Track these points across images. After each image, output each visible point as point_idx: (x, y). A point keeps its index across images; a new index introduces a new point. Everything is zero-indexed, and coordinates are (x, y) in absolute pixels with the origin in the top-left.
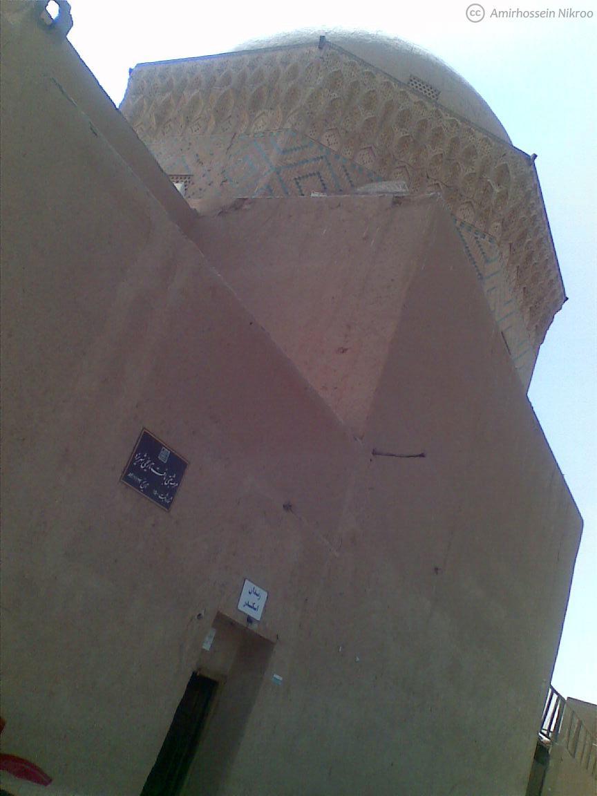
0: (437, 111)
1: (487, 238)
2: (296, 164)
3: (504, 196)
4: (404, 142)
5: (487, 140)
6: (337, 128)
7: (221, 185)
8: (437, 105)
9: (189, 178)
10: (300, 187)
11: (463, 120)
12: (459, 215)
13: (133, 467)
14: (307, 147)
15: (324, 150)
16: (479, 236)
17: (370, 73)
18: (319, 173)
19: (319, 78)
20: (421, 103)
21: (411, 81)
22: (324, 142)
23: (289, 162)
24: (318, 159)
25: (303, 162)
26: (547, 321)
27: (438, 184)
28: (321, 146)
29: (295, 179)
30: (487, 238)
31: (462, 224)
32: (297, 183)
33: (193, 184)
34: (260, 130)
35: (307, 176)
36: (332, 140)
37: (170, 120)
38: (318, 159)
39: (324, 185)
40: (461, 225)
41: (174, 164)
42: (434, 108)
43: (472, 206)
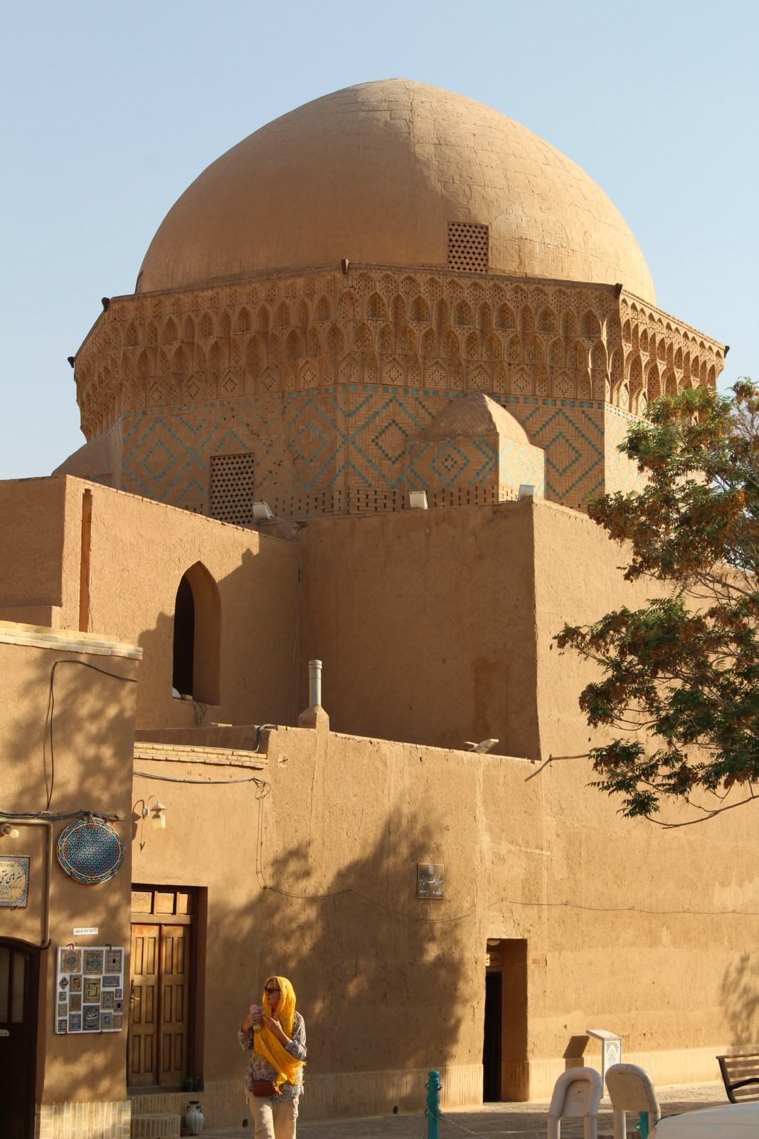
0: (495, 285)
2: (367, 424)
5: (560, 291)
6: (394, 359)
7: (294, 464)
8: (494, 277)
9: (250, 456)
10: (380, 448)
12: (557, 393)
14: (371, 396)
15: (390, 390)
16: (585, 408)
17: (409, 278)
18: (394, 421)
19: (356, 309)
21: (451, 230)
22: (387, 381)
23: (361, 423)
24: (388, 404)
25: (374, 417)
27: (522, 368)
29: (373, 441)
32: (377, 444)
33: (258, 464)
34: (311, 385)
35: (384, 431)
36: (394, 374)
37: (192, 376)
38: (388, 404)
39: (404, 432)
40: (562, 405)
41: (224, 440)
42: (492, 283)
43: (567, 375)
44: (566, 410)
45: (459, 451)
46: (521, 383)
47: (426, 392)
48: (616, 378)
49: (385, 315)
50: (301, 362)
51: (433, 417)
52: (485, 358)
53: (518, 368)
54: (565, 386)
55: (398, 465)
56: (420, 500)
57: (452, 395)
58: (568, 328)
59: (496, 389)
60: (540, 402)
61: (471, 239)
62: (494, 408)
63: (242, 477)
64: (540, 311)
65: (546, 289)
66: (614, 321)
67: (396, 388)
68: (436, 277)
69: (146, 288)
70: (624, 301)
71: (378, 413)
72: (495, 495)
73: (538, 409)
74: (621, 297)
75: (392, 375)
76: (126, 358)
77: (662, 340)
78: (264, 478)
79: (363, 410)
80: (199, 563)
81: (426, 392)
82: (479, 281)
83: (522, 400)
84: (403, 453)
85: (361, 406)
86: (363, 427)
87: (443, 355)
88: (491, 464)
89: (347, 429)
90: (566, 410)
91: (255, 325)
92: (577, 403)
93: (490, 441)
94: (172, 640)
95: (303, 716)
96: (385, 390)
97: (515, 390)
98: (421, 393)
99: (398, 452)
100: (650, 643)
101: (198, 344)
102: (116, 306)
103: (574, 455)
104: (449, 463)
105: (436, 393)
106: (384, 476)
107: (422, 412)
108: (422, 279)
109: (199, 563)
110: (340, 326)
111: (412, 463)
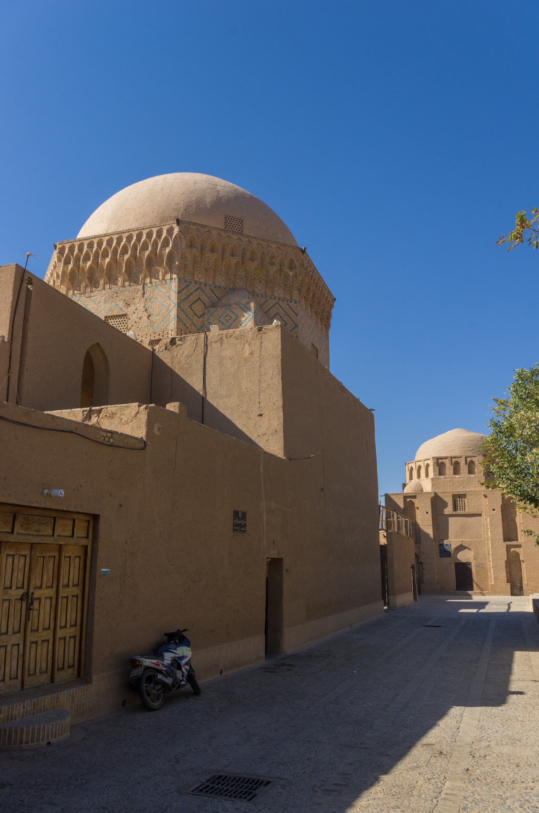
0: (249, 240)
1: (293, 302)
2: (187, 298)
3: (295, 276)
4: (237, 264)
5: (278, 247)
8: (248, 236)
11: (264, 240)
12: (276, 294)
13: (235, 525)
14: (188, 285)
16: (289, 303)
17: (208, 231)
18: (200, 298)
20: (239, 239)
24: (197, 290)
25: (190, 295)
26: (329, 317)
30: (293, 302)
31: (279, 299)
32: (191, 308)
33: (129, 319)
36: (200, 276)
38: (197, 290)
42: (247, 239)
44: (281, 303)
45: (233, 312)
51: (218, 299)
52: (243, 274)
53: (258, 281)
55: (201, 319)
58: (281, 265)
59: (248, 289)
60: (268, 298)
63: (120, 325)
67: (200, 284)
68: (221, 232)
71: (192, 294)
78: (132, 326)
82: (242, 237)
83: (260, 296)
84: (204, 314)
85: (183, 289)
88: (250, 318)
90: (281, 303)
96: (196, 283)
97: (257, 291)
98: (213, 287)
99: (201, 313)
104: (228, 318)
106: (194, 324)
107: (213, 295)
108: (214, 232)
109: (98, 344)
111: (208, 319)
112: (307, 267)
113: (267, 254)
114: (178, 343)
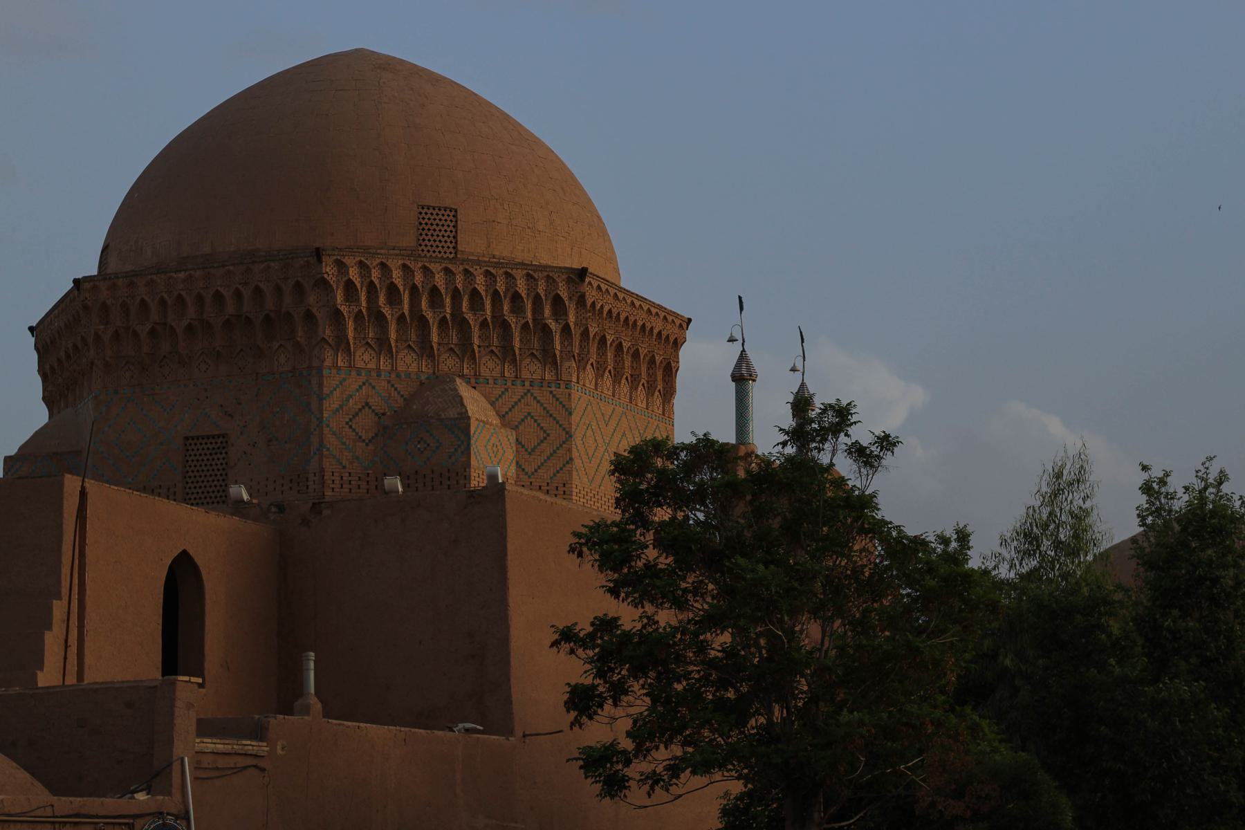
1: (563, 386)
2: (341, 407)
8: (463, 262)
12: (525, 374)
18: (367, 404)
22: (360, 364)
23: (336, 406)
24: (361, 387)
28: (359, 370)
30: (563, 386)
38: (361, 387)
42: (461, 268)
44: (536, 391)
46: (490, 364)
47: (398, 376)
48: (582, 363)
49: (358, 300)
50: (276, 345)
52: (455, 340)
54: (532, 368)
55: (371, 447)
56: (396, 483)
57: (423, 377)
60: (509, 384)
61: (439, 223)
62: (464, 390)
64: (509, 295)
65: (514, 272)
66: (581, 300)
67: (370, 371)
69: (113, 266)
70: (590, 283)
72: (467, 478)
73: (506, 390)
74: (587, 280)
75: (364, 358)
76: (97, 337)
77: (627, 318)
79: (337, 394)
80: (184, 551)
81: (398, 376)
83: (491, 381)
86: (337, 410)
87: (414, 337)
89: (321, 412)
90: (536, 391)
91: (230, 308)
92: (545, 384)
93: (461, 425)
94: (160, 628)
95: (298, 704)
98: (393, 376)
99: (371, 435)
100: (611, 650)
101: (171, 327)
102: (87, 286)
103: (542, 435)
105: (408, 375)
106: (357, 458)
107: (394, 394)
109: (184, 551)
110: (314, 311)
112: (593, 304)
113: (505, 293)
114: (326, 512)
